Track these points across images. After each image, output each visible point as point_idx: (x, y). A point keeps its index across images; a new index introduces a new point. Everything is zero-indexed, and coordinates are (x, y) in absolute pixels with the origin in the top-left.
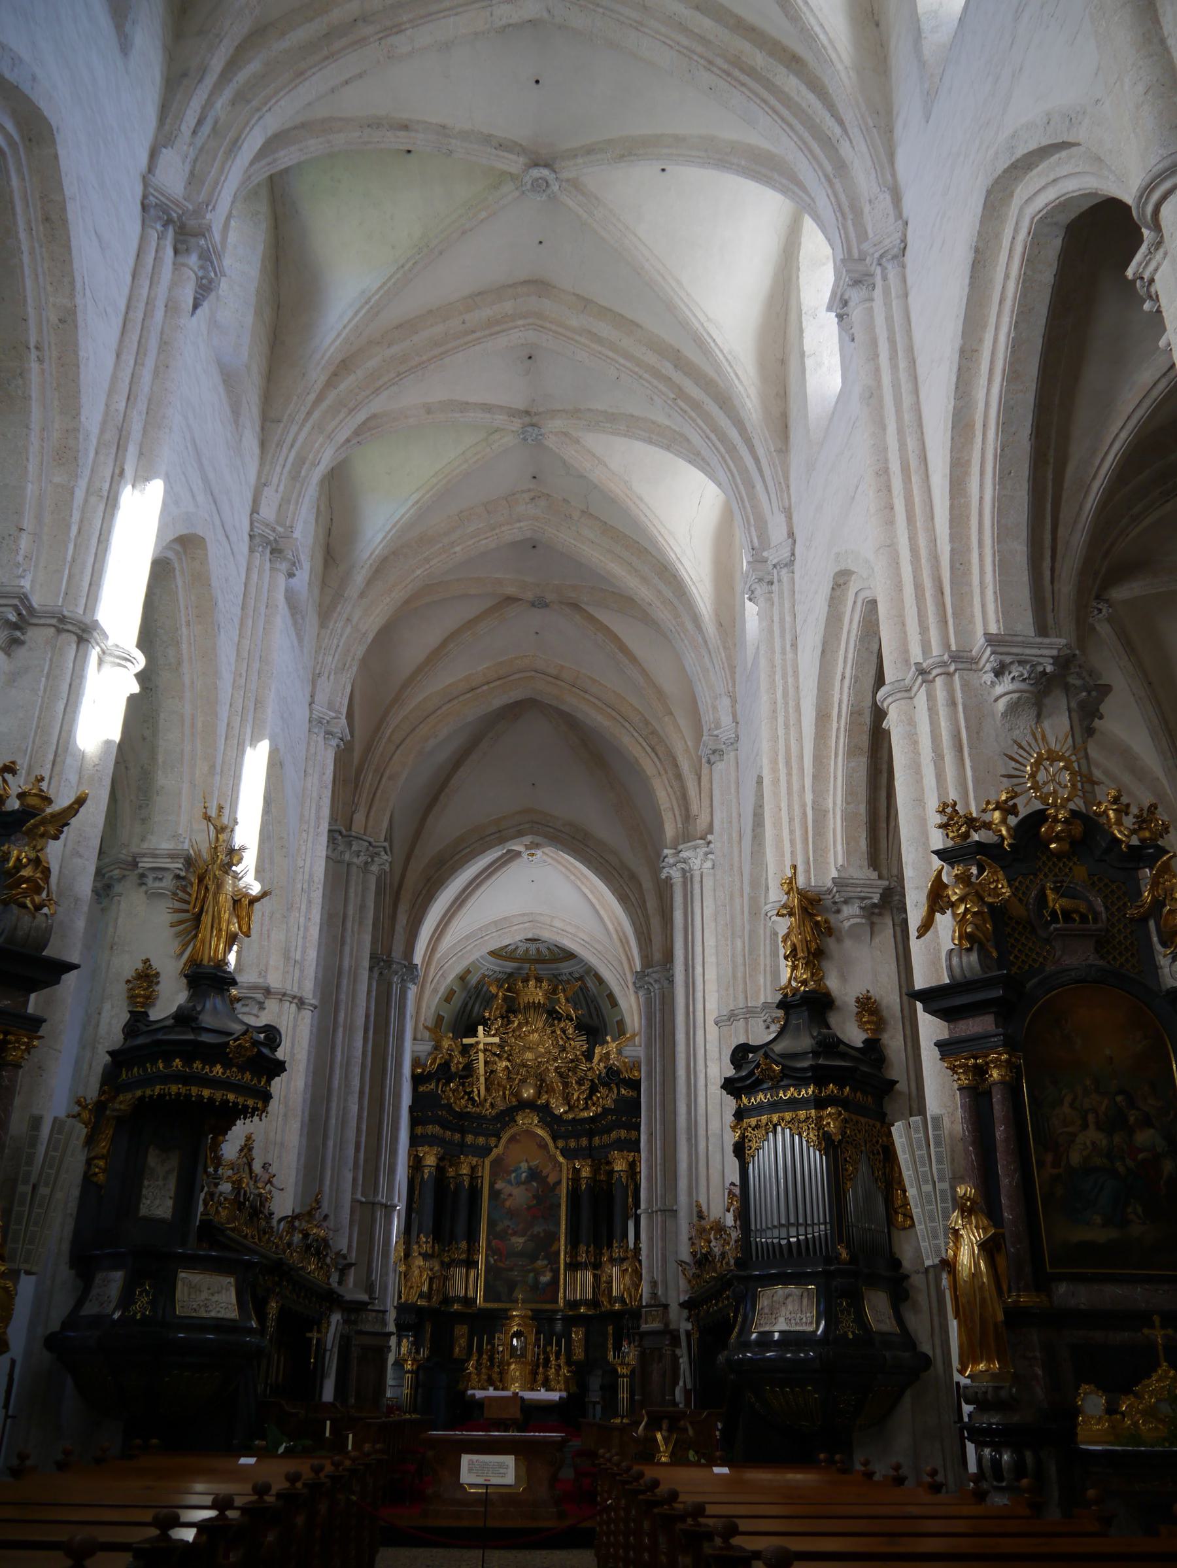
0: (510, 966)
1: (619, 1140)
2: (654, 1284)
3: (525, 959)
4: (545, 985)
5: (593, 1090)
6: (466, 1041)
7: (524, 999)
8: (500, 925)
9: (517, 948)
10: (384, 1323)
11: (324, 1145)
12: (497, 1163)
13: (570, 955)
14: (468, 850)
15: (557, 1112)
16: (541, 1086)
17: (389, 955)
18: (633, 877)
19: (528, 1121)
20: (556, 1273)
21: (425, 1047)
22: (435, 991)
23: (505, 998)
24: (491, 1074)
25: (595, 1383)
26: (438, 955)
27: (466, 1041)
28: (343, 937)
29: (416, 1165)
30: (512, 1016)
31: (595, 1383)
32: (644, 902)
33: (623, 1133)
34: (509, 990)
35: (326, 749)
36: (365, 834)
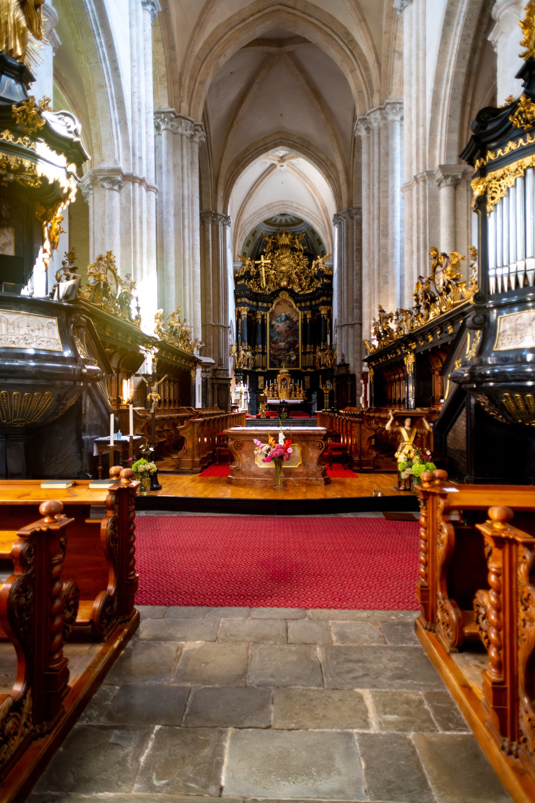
0: (273, 229)
1: (323, 301)
2: (343, 355)
3: (280, 225)
4: (290, 236)
5: (312, 281)
6: (256, 262)
7: (281, 242)
8: (269, 207)
9: (276, 220)
10: (228, 375)
11: (184, 288)
12: (272, 314)
13: (300, 221)
14: (250, 156)
15: (296, 291)
16: (289, 281)
17: (216, 211)
18: (333, 165)
19: (284, 296)
20: (298, 356)
21: (239, 265)
22: (241, 240)
23: (272, 243)
24: (267, 276)
25: (314, 396)
26: (241, 223)
27: (256, 262)
28: (182, 178)
29: (238, 315)
30: (275, 251)
31: (314, 396)
32: (339, 178)
33: (325, 298)
34: (274, 239)
35: (144, 12)
36: (189, 115)
